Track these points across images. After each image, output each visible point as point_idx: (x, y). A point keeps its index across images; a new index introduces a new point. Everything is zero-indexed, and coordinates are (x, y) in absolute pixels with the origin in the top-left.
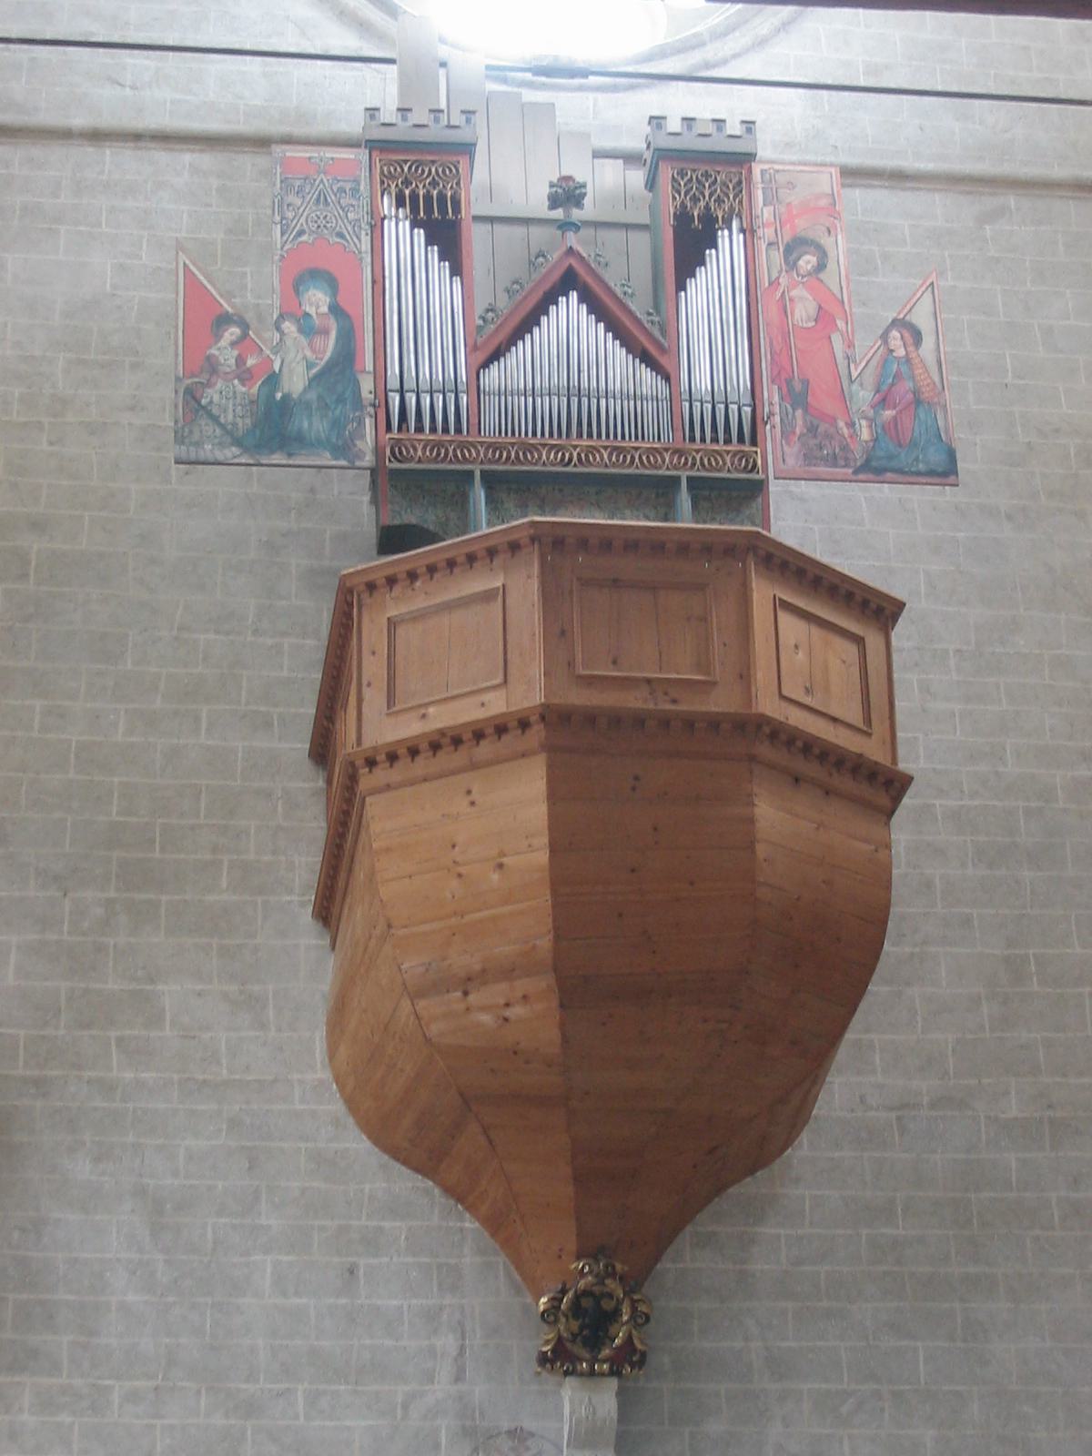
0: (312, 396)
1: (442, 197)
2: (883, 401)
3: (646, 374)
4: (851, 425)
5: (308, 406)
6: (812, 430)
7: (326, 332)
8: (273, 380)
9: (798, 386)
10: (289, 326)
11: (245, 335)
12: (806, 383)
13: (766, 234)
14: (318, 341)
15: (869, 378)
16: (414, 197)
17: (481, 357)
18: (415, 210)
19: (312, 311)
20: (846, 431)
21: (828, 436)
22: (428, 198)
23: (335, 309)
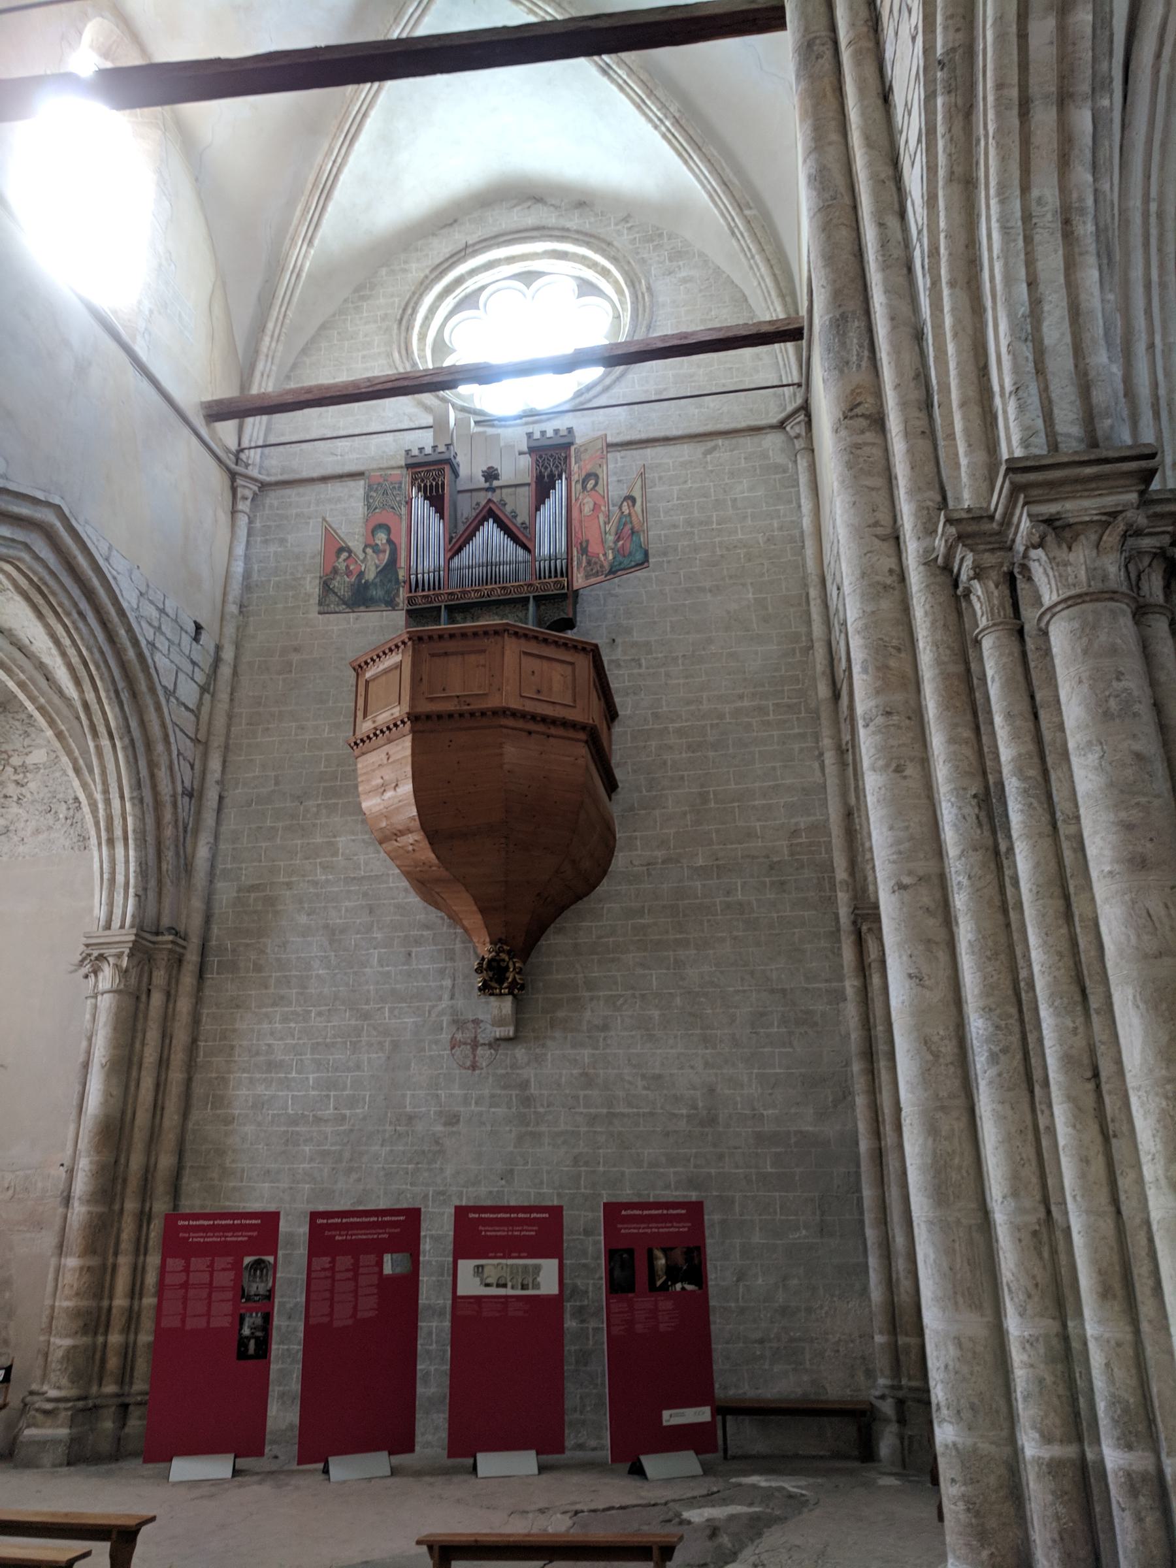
0: (378, 580)
1: (437, 484)
2: (618, 540)
3: (520, 551)
4: (605, 555)
5: (375, 585)
6: (589, 563)
7: (384, 551)
8: (361, 574)
9: (584, 545)
10: (369, 551)
11: (350, 556)
12: (587, 541)
13: (575, 477)
14: (381, 556)
15: (613, 530)
16: (425, 486)
17: (449, 555)
18: (425, 492)
19: (379, 542)
20: (602, 558)
21: (596, 563)
22: (431, 485)
23: (389, 541)
